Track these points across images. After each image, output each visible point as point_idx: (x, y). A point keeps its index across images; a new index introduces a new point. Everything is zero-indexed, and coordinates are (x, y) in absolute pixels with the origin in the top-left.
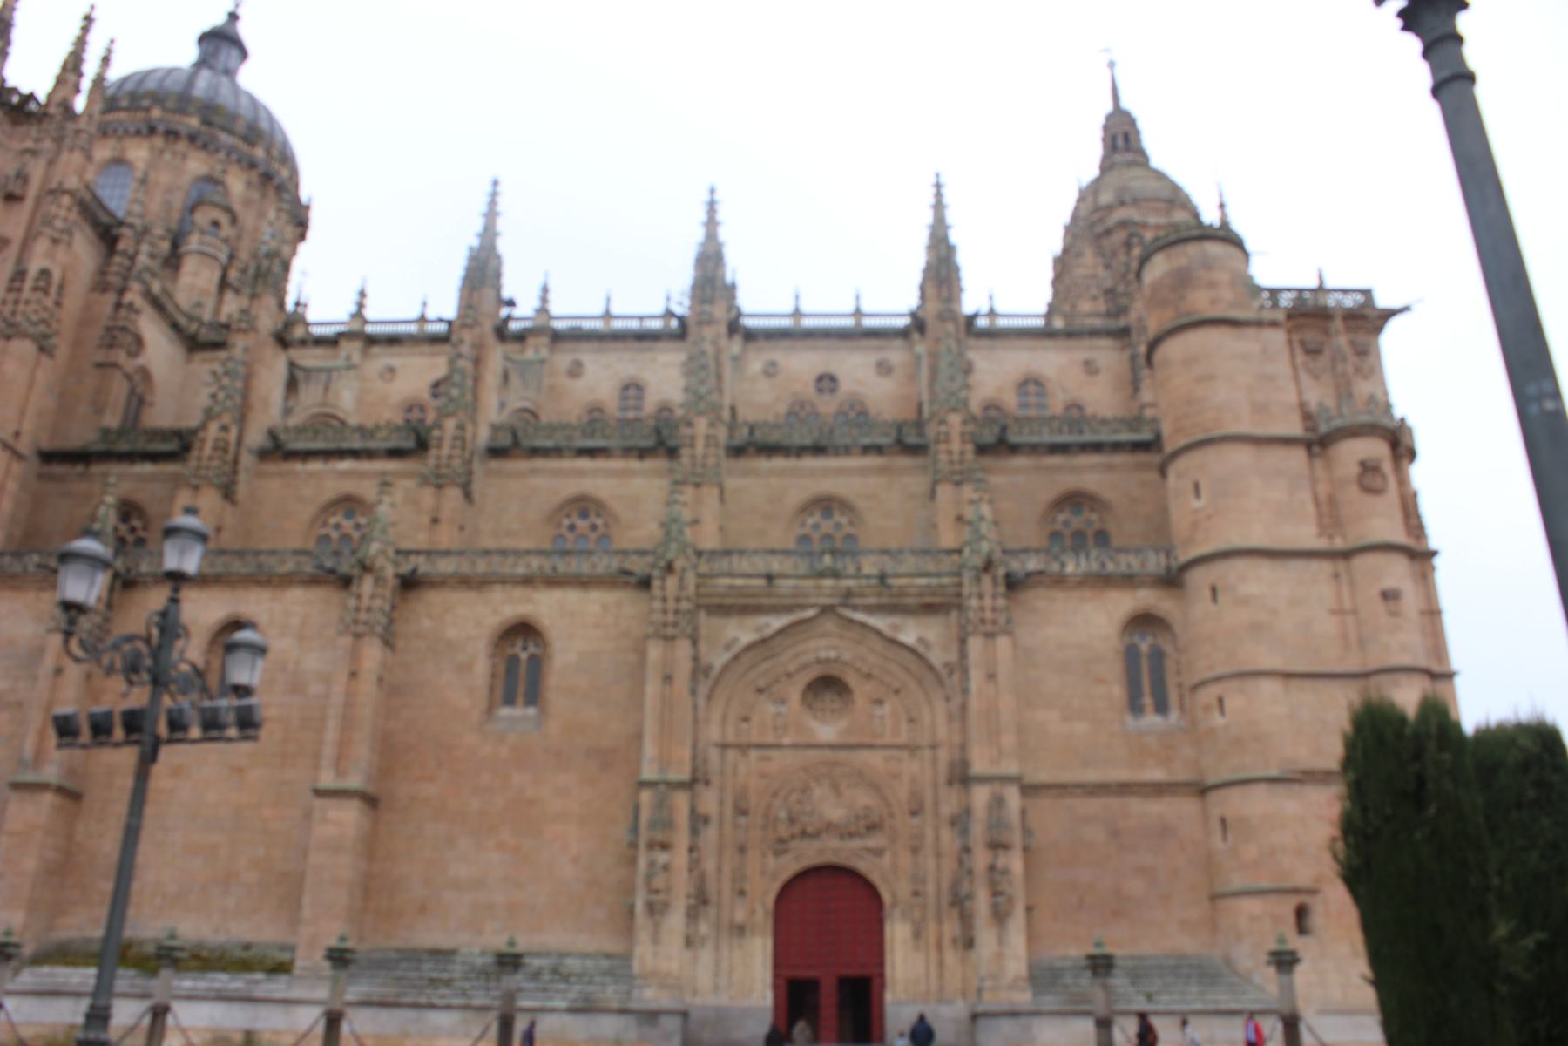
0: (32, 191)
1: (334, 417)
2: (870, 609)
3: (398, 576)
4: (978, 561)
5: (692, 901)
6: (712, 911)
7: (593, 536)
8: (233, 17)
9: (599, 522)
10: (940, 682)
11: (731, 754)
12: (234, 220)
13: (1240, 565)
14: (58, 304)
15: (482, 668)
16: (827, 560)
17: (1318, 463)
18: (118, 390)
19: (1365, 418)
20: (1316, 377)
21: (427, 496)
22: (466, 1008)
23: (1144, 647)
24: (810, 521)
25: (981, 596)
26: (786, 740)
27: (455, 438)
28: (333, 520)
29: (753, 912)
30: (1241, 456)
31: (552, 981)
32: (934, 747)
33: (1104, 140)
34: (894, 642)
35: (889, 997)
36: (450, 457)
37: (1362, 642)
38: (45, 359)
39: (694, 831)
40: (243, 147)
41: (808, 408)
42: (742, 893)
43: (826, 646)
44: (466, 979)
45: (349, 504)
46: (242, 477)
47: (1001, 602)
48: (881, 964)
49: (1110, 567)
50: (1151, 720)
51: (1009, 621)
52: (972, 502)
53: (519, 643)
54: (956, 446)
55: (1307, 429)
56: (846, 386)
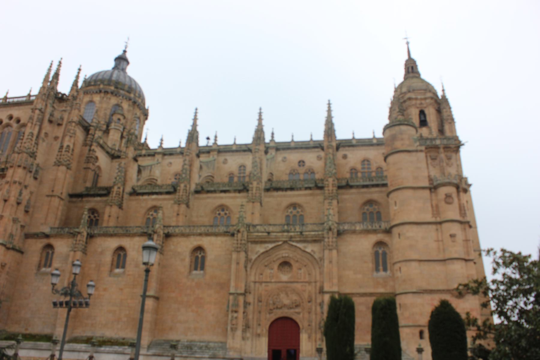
0: (64, 123)
1: (154, 179)
2: (298, 242)
3: (164, 233)
4: (327, 227)
5: (244, 327)
6: (251, 330)
7: (225, 217)
8: (125, 52)
9: (227, 212)
10: (318, 263)
11: (257, 285)
12: (125, 118)
13: (407, 227)
14: (72, 155)
15: (188, 260)
16: (286, 227)
17: (433, 194)
18: (91, 175)
19: (447, 181)
20: (434, 167)
21: (176, 207)
22: (181, 357)
23: (380, 251)
24: (290, 211)
25: (328, 238)
26: (273, 281)
27: (184, 190)
28: (151, 213)
29: (262, 330)
30: (409, 193)
31: (205, 349)
32: (316, 282)
33: (405, 69)
34: (304, 251)
35: (301, 355)
36: (182, 195)
37: (444, 250)
38: (69, 171)
39: (245, 307)
40: (127, 94)
41: (296, 171)
42: (259, 325)
43: (285, 253)
44: (182, 349)
45: (155, 208)
46: (125, 202)
47: (334, 240)
48: (299, 346)
49: (370, 227)
50: (382, 273)
51: (337, 246)
52: (328, 209)
53: (199, 252)
54: (331, 188)
55: (430, 184)
56: (307, 164)
